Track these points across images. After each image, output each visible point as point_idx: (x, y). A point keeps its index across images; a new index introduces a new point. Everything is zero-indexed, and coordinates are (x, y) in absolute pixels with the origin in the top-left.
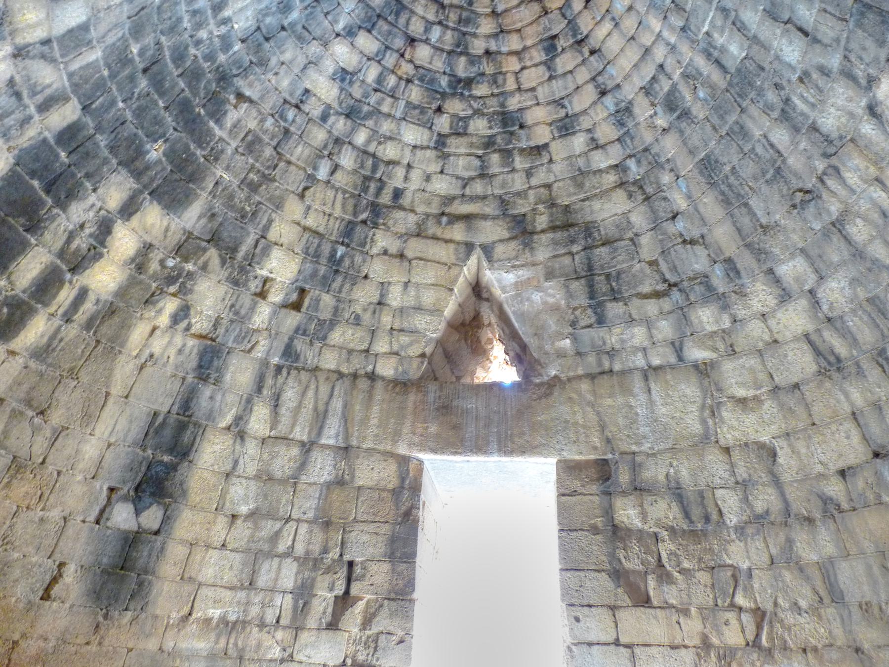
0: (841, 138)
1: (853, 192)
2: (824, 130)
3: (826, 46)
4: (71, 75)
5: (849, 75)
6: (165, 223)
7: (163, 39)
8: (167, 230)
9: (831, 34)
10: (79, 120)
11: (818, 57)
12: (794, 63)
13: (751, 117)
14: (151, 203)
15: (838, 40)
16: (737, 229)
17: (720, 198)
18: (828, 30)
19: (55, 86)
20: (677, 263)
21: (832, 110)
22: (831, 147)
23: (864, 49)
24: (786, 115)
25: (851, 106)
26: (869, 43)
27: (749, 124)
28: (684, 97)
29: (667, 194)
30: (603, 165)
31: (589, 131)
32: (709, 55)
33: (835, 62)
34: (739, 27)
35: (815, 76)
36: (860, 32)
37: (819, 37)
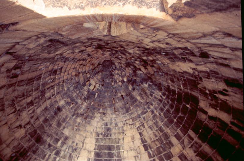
0: (19, 115)
1: (8, 115)
2: (24, 111)
3: (35, 120)
4: (184, 135)
5: (29, 123)
6: (201, 101)
7: (171, 112)
8: (202, 100)
9: (36, 123)
10: (191, 129)
11: (35, 118)
12: (37, 109)
13: (37, 93)
14: (199, 106)
15: (34, 124)
16: (22, 81)
17: (32, 78)
18: (37, 123)
19: (187, 138)
20: (33, 61)
21: (26, 116)
22: (18, 112)
23: (30, 129)
24: (31, 103)
25: (23, 121)
26: (30, 131)
27: (36, 92)
28: (53, 76)
29: (46, 64)
30: (68, 51)
31: (75, 53)
32: (52, 86)
33: (32, 121)
34: (50, 98)
35: (33, 114)
36: (33, 130)
37: (37, 120)
